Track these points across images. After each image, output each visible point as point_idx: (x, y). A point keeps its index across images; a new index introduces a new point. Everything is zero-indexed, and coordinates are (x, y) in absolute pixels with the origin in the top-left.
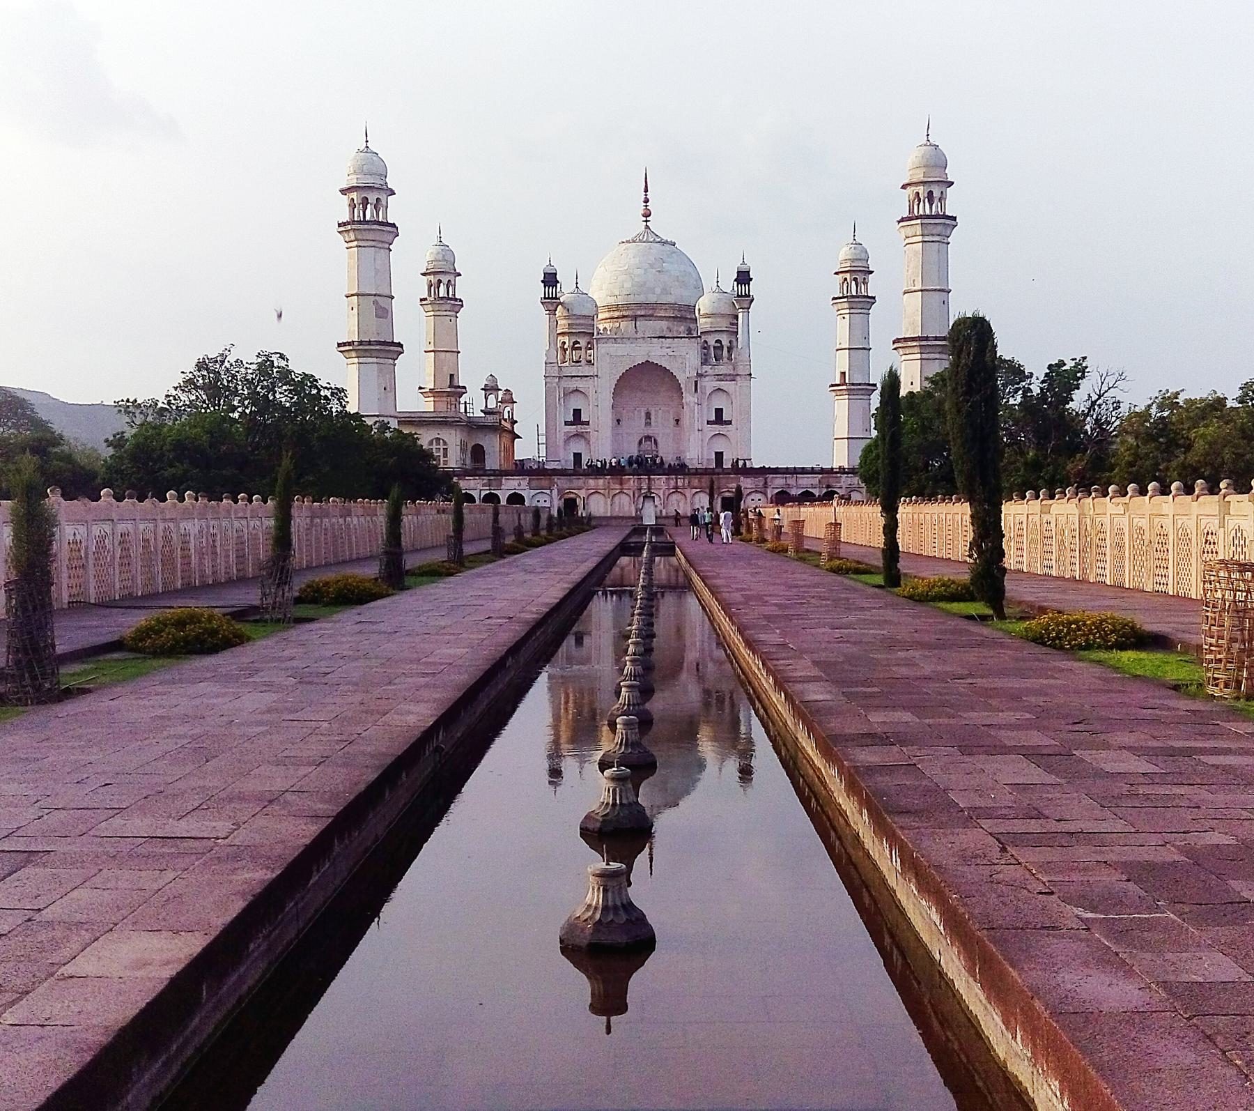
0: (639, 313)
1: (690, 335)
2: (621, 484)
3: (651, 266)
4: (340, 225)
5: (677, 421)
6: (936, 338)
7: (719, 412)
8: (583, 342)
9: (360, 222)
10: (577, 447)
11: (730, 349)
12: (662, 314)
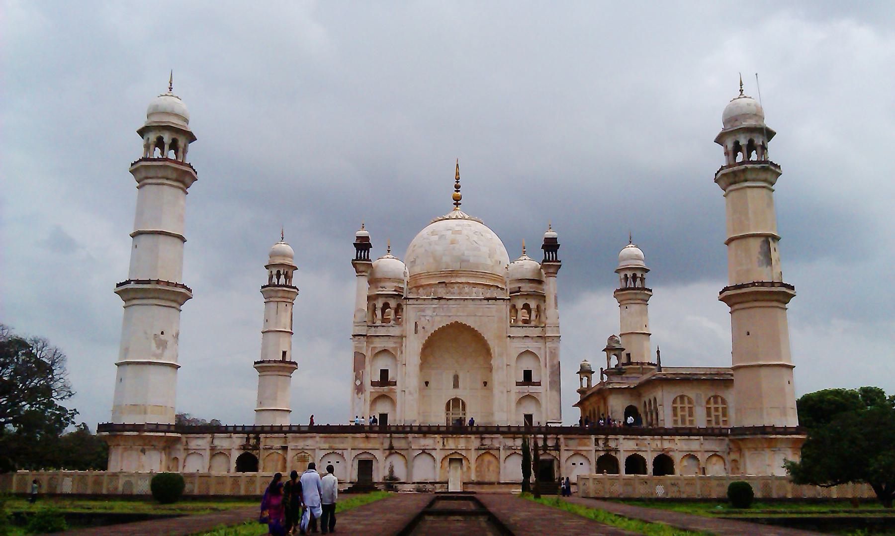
5: (485, 384)
7: (528, 374)
8: (393, 303)
10: (383, 408)
11: (538, 315)
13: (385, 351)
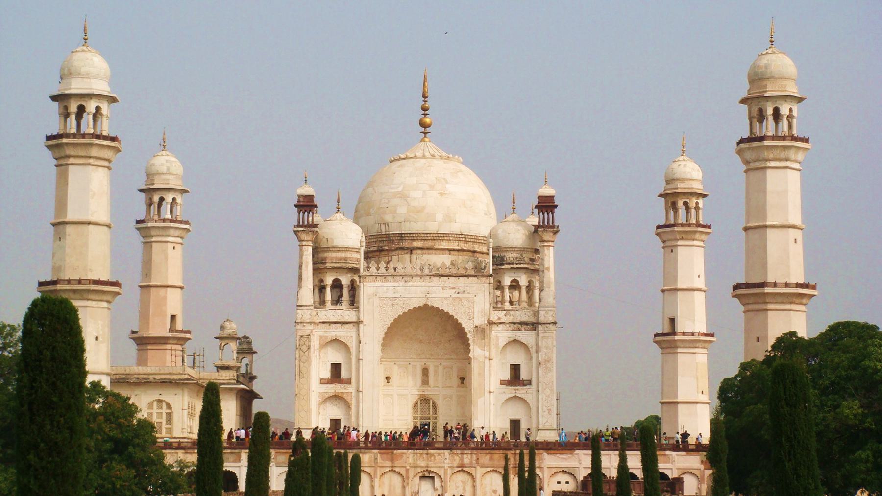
0: (415, 244)
1: (479, 271)
2: (392, 461)
3: (432, 187)
4: (49, 138)
5: (462, 379)
6: (787, 285)
9: (74, 136)
12: (444, 245)
13: (336, 341)
